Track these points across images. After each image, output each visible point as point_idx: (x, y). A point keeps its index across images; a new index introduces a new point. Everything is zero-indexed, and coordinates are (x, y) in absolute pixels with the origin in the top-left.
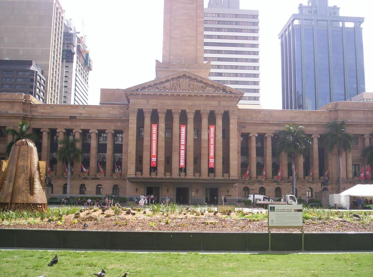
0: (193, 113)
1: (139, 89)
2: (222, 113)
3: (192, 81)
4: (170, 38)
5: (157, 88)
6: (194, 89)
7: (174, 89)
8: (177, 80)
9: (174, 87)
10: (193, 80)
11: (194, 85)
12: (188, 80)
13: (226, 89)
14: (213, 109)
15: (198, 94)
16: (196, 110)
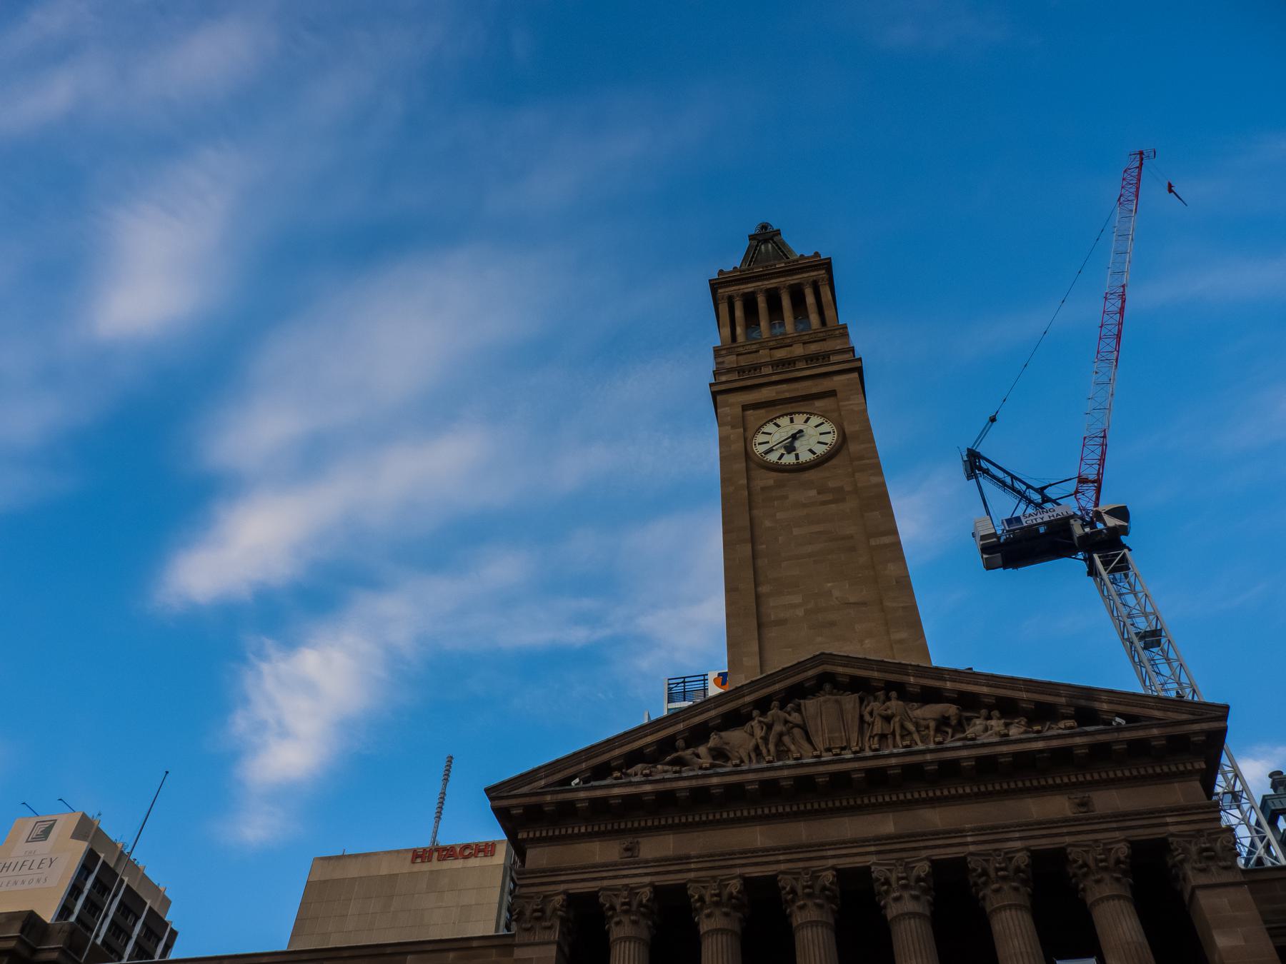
0: (919, 879)
2: (1118, 861)
3: (876, 699)
5: (680, 762)
6: (898, 738)
7: (772, 747)
9: (772, 739)
10: (881, 694)
11: (888, 719)
12: (850, 701)
13: (1097, 705)
14: (1045, 844)
15: (929, 757)
16: (935, 863)
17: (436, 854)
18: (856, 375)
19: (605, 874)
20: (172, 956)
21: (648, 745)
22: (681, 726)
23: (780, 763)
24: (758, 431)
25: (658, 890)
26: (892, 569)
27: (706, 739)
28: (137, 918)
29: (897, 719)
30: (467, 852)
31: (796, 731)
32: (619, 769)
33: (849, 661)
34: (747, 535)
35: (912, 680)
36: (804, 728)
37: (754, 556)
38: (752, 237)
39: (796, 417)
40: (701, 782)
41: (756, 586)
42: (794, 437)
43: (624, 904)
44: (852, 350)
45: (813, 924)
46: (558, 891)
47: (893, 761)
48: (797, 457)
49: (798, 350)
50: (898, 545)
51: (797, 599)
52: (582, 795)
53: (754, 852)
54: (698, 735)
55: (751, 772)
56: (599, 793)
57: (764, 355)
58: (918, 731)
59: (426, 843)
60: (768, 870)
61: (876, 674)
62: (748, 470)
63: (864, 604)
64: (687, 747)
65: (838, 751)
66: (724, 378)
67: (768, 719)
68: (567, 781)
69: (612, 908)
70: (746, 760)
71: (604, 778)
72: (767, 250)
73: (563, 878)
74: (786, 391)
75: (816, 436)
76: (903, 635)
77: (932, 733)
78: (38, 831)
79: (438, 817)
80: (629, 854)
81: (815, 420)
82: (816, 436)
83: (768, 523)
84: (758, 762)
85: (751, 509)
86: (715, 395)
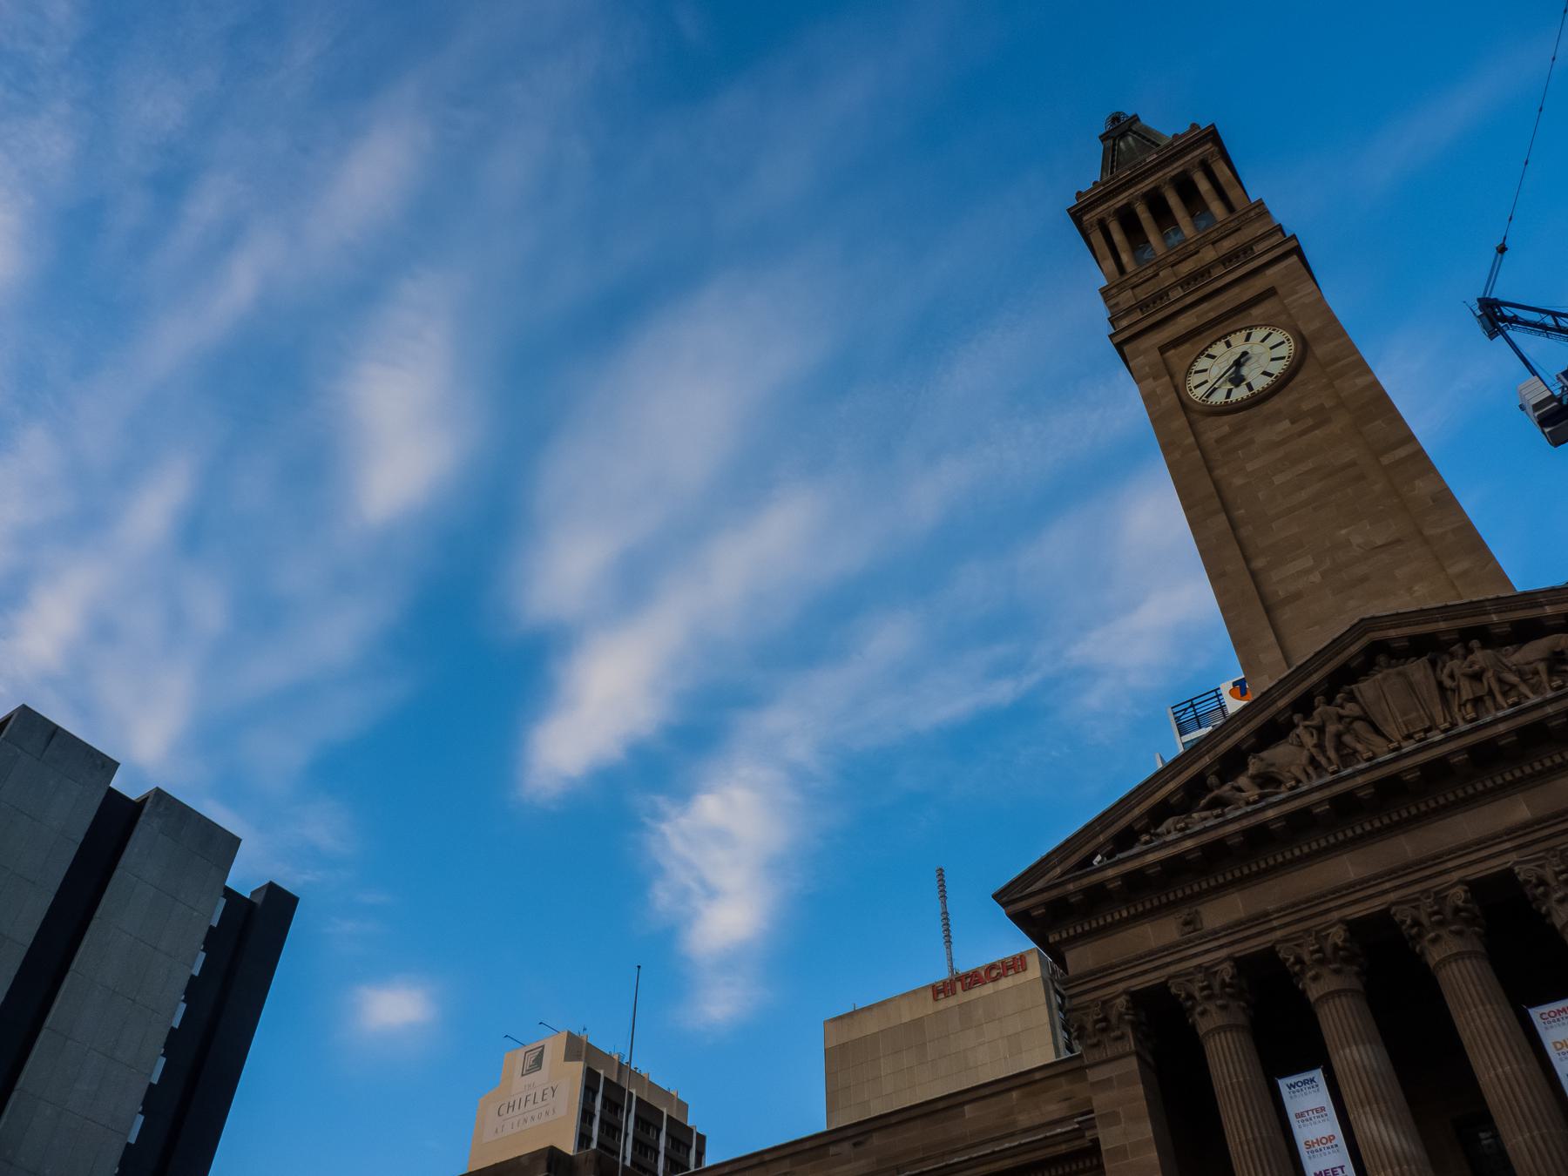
1: (1094, 855)
3: (1453, 656)
4: (1268, 610)
5: (1220, 803)
6: (1499, 698)
7: (1332, 754)
8: (1339, 697)
10: (1457, 648)
11: (1477, 677)
12: (1418, 670)
15: (1549, 710)
17: (959, 985)
18: (1295, 258)
19: (1168, 959)
20: (708, 1162)
21: (1172, 793)
22: (1207, 760)
23: (1349, 770)
24: (1188, 372)
25: (1240, 963)
26: (1422, 487)
27: (1244, 767)
28: (659, 1130)
29: (1490, 674)
30: (994, 974)
31: (1358, 725)
32: (1147, 831)
33: (1399, 619)
34: (1216, 504)
35: (1495, 618)
36: (1366, 718)
37: (1234, 526)
38: (1104, 138)
39: (1232, 339)
40: (1253, 820)
41: (1247, 560)
42: (1238, 364)
43: (1202, 989)
44: (1280, 228)
45: (1458, 956)
46: (1116, 993)
47: (1502, 728)
48: (1250, 387)
49: (1209, 254)
50: (1420, 454)
51: (1308, 562)
52: (1110, 873)
53: (1351, 887)
54: (1232, 763)
55: (1315, 791)
56: (1129, 866)
57: (1167, 277)
58: (1524, 681)
59: (943, 975)
60: (1376, 905)
61: (1442, 625)
62: (1191, 424)
63: (1398, 541)
64: (1223, 782)
65: (1422, 735)
66: (1124, 323)
67: (1316, 721)
68: (1087, 861)
69: (1190, 996)
70: (1303, 778)
71: (1131, 847)
72: (1127, 144)
73: (1118, 976)
74: (1208, 310)
75: (1266, 353)
76: (1464, 565)
77: (1544, 677)
78: (531, 1058)
79: (948, 942)
80: (1190, 928)
81: (1259, 334)
82: (1266, 353)
83: (1238, 481)
84: (1320, 776)
85: (1210, 470)
86: (1119, 347)
